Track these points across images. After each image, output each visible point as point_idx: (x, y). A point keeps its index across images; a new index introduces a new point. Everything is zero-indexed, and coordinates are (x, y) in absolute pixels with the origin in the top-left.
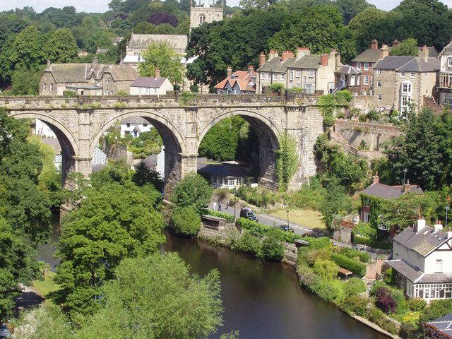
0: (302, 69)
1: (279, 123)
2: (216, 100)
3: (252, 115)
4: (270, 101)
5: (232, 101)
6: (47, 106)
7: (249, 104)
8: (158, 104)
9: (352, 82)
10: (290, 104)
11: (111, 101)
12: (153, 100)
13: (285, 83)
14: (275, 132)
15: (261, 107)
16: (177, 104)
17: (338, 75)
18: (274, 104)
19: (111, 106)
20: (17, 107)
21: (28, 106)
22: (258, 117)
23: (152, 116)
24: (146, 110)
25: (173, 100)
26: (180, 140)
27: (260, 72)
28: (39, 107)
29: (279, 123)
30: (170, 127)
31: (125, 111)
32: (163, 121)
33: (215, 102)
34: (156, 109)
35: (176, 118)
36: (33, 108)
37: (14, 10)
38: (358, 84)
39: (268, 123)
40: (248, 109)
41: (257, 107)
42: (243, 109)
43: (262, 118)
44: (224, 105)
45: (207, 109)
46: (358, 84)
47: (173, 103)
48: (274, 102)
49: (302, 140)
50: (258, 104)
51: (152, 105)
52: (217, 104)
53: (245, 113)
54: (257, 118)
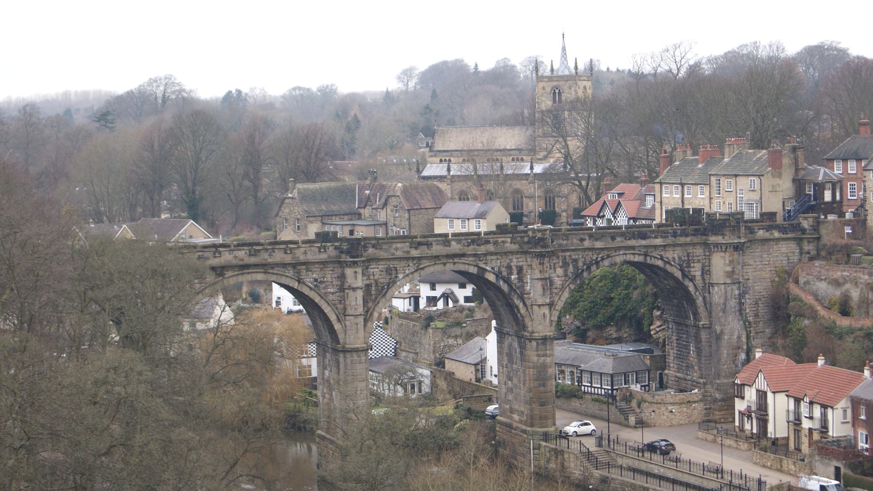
0: (736, 176)
2: (582, 236)
4: (681, 235)
5: (613, 239)
6: (288, 259)
7: (643, 242)
8: (482, 249)
9: (828, 196)
10: (719, 239)
11: (399, 245)
12: (473, 242)
13: (707, 202)
14: (691, 288)
15: (665, 246)
16: (515, 247)
17: (799, 184)
18: (688, 239)
19: (399, 254)
20: (234, 262)
21: (253, 260)
23: (473, 270)
25: (509, 240)
26: (523, 310)
27: (661, 183)
28: (270, 260)
30: (505, 287)
32: (491, 277)
33: (582, 240)
35: (515, 271)
36: (264, 262)
37: (234, 91)
38: (838, 198)
41: (655, 247)
42: (632, 252)
44: (599, 245)
46: (838, 198)
47: (508, 245)
48: (687, 235)
49: (741, 304)
50: (658, 241)
51: (470, 250)
52: (587, 244)
54: (658, 267)
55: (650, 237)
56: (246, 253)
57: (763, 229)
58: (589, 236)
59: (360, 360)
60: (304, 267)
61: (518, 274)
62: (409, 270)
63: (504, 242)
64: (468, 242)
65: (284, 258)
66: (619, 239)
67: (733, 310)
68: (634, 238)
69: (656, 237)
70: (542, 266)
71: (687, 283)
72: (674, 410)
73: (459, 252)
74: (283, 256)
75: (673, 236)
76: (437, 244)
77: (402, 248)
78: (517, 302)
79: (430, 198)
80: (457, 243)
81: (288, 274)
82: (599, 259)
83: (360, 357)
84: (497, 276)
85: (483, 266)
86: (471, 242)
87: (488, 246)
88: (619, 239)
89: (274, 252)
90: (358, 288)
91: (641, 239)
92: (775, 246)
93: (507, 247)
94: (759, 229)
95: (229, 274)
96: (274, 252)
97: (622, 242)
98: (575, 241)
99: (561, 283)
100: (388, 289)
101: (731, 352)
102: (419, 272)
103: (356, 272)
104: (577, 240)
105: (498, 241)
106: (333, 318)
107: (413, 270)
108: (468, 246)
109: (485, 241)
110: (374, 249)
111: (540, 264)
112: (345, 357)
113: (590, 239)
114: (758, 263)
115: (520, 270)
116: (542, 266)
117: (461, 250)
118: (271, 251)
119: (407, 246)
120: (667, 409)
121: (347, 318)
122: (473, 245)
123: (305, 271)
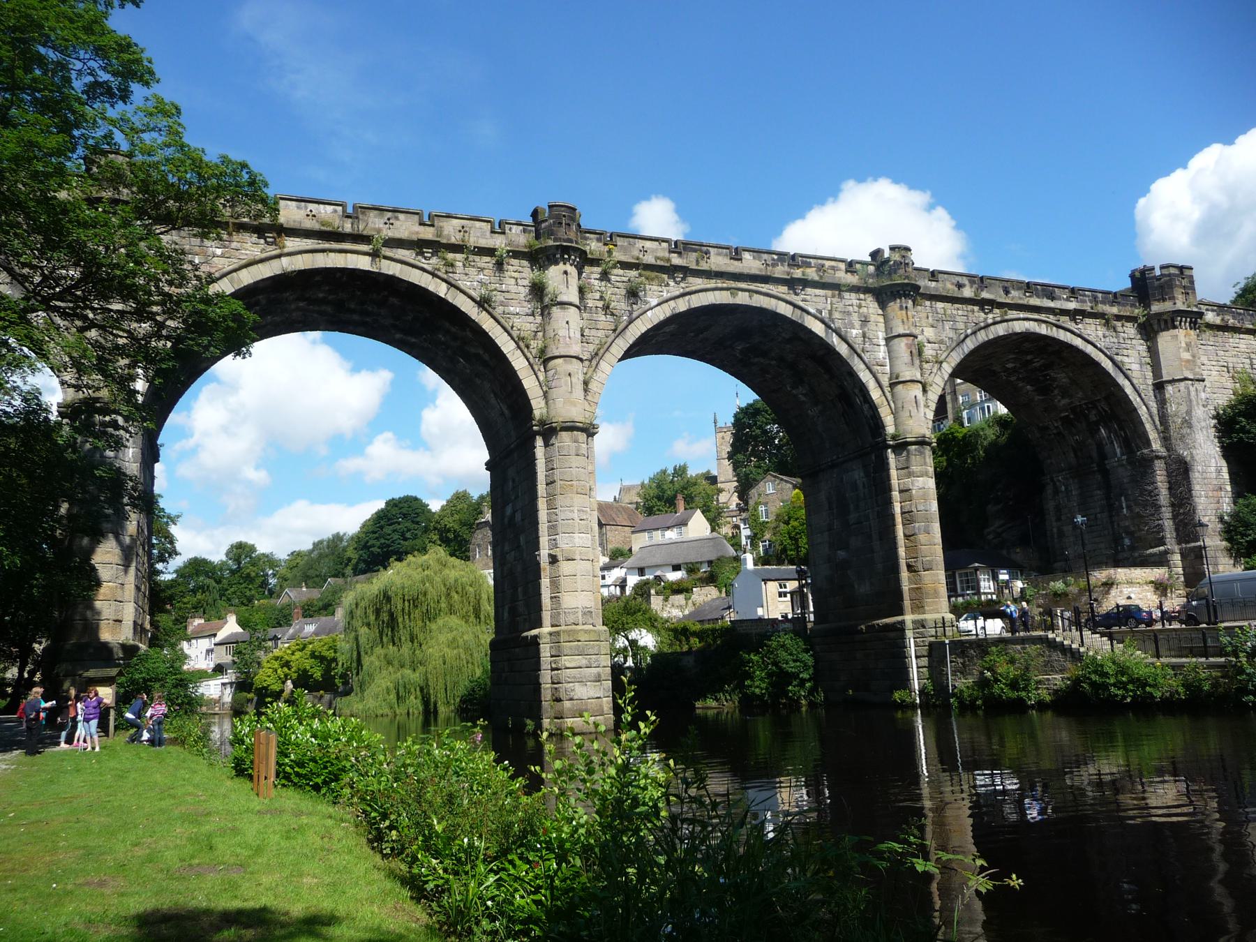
1: (1135, 367)
3: (1063, 336)
4: (1103, 302)
20: (309, 224)
22: (1078, 342)
24: (765, 288)
26: (875, 394)
29: (1135, 367)
30: (843, 349)
31: (698, 283)
32: (818, 328)
33: (960, 286)
34: (792, 283)
35: (855, 318)
39: (1107, 364)
40: (1052, 318)
42: (1036, 316)
43: (1089, 349)
45: (940, 305)
52: (968, 292)
53: (1043, 330)
55: (1059, 298)
56: (335, 211)
57: (1213, 311)
58: (970, 281)
59: (578, 448)
60: (459, 256)
61: (862, 327)
62: (668, 292)
63: (833, 268)
64: (773, 259)
65: (417, 233)
66: (1014, 293)
67: (1203, 424)
68: (1038, 297)
69: (1068, 299)
70: (904, 312)
71: (1121, 380)
72: (1132, 596)
73: (754, 272)
74: (417, 228)
75: (1091, 302)
76: (719, 254)
77: (654, 251)
78: (865, 376)
79: (626, 517)
80: (754, 258)
81: (425, 266)
82: (990, 321)
83: (576, 441)
84: (828, 326)
85: (801, 304)
86: (778, 260)
87: (809, 271)
88: (1014, 293)
89: (397, 218)
90: (571, 304)
91: (1048, 298)
92: (1231, 340)
93: (840, 278)
94: (1207, 310)
95: (292, 244)
96: (397, 218)
97: (1020, 298)
98: (949, 286)
99: (934, 353)
100: (630, 322)
101: (1210, 494)
102: (687, 298)
103: (566, 273)
104: (953, 284)
105: (823, 266)
106: (519, 363)
107: (678, 293)
108: (774, 265)
109: (802, 262)
110: (601, 244)
111: (901, 308)
112: (547, 445)
113: (971, 287)
114: (1214, 363)
115: (865, 321)
116: (904, 312)
117: (761, 270)
118: (389, 215)
119: (663, 249)
120: (1121, 592)
121: (552, 364)
122: (782, 265)
123: (461, 264)
